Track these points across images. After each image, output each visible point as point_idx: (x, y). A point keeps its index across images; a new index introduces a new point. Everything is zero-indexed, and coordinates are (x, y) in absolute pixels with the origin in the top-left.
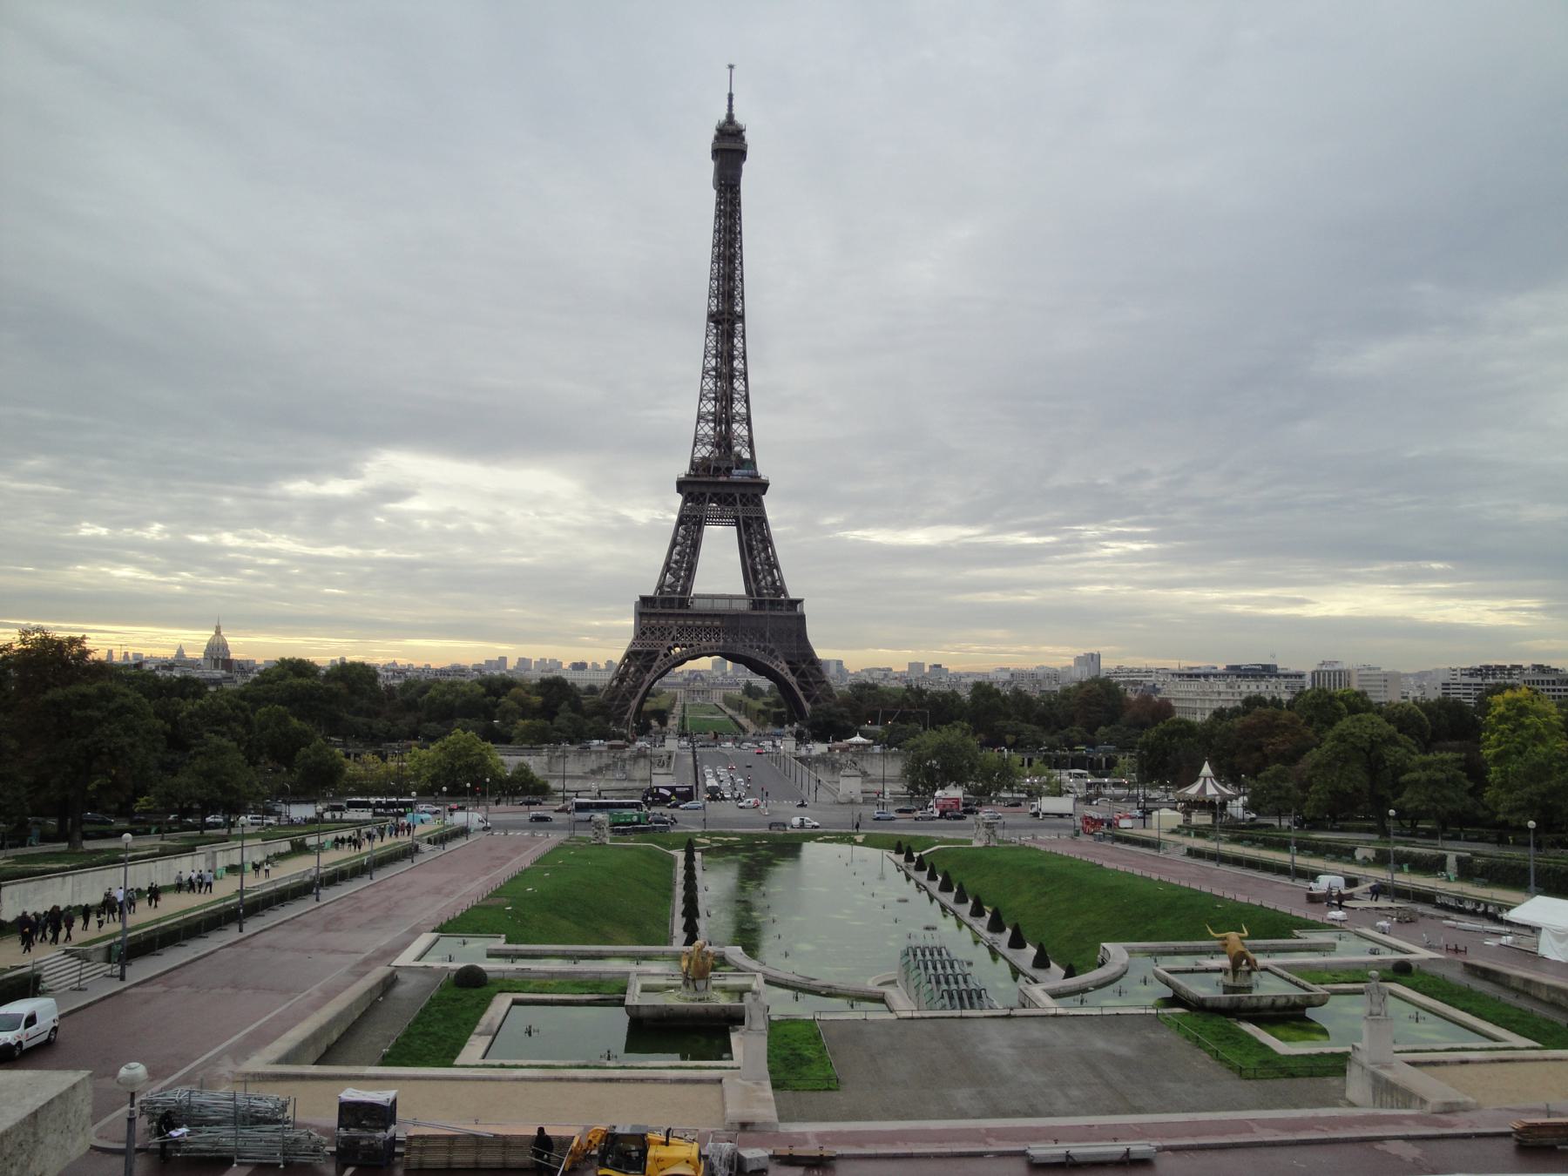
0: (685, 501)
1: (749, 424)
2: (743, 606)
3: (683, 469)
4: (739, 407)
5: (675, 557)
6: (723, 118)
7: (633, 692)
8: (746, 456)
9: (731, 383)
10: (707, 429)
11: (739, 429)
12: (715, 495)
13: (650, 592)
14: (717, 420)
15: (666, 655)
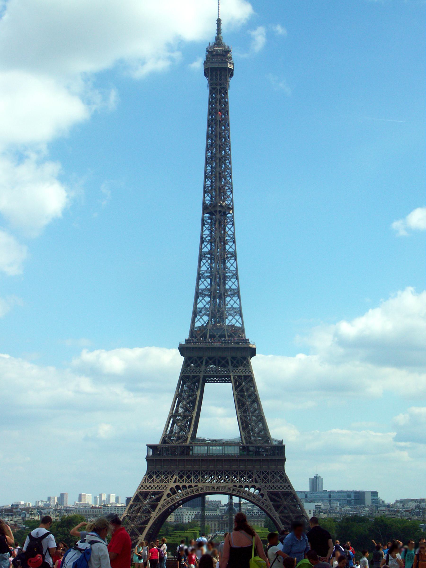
0: (186, 364)
1: (239, 297)
2: (234, 451)
3: (184, 336)
4: (230, 284)
5: (181, 410)
6: (212, 40)
7: (141, 530)
8: (238, 325)
9: (224, 264)
10: (204, 302)
11: (231, 302)
12: (210, 358)
13: (157, 441)
14: (213, 295)
15: (168, 495)
